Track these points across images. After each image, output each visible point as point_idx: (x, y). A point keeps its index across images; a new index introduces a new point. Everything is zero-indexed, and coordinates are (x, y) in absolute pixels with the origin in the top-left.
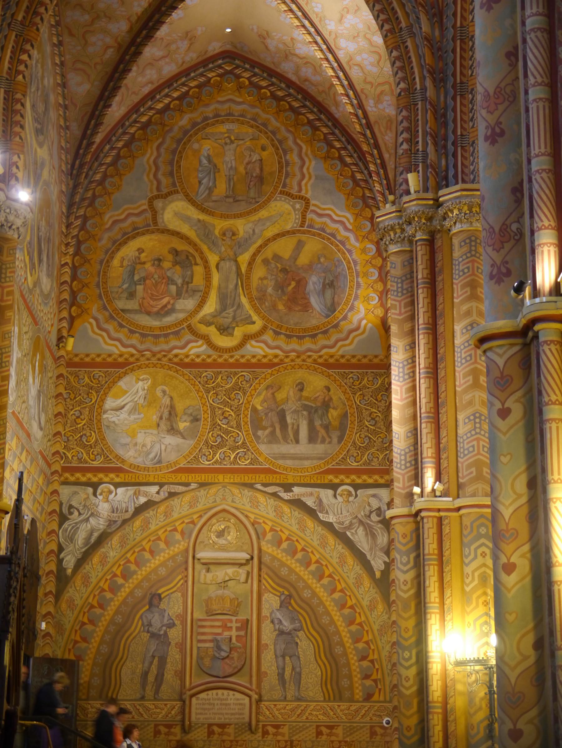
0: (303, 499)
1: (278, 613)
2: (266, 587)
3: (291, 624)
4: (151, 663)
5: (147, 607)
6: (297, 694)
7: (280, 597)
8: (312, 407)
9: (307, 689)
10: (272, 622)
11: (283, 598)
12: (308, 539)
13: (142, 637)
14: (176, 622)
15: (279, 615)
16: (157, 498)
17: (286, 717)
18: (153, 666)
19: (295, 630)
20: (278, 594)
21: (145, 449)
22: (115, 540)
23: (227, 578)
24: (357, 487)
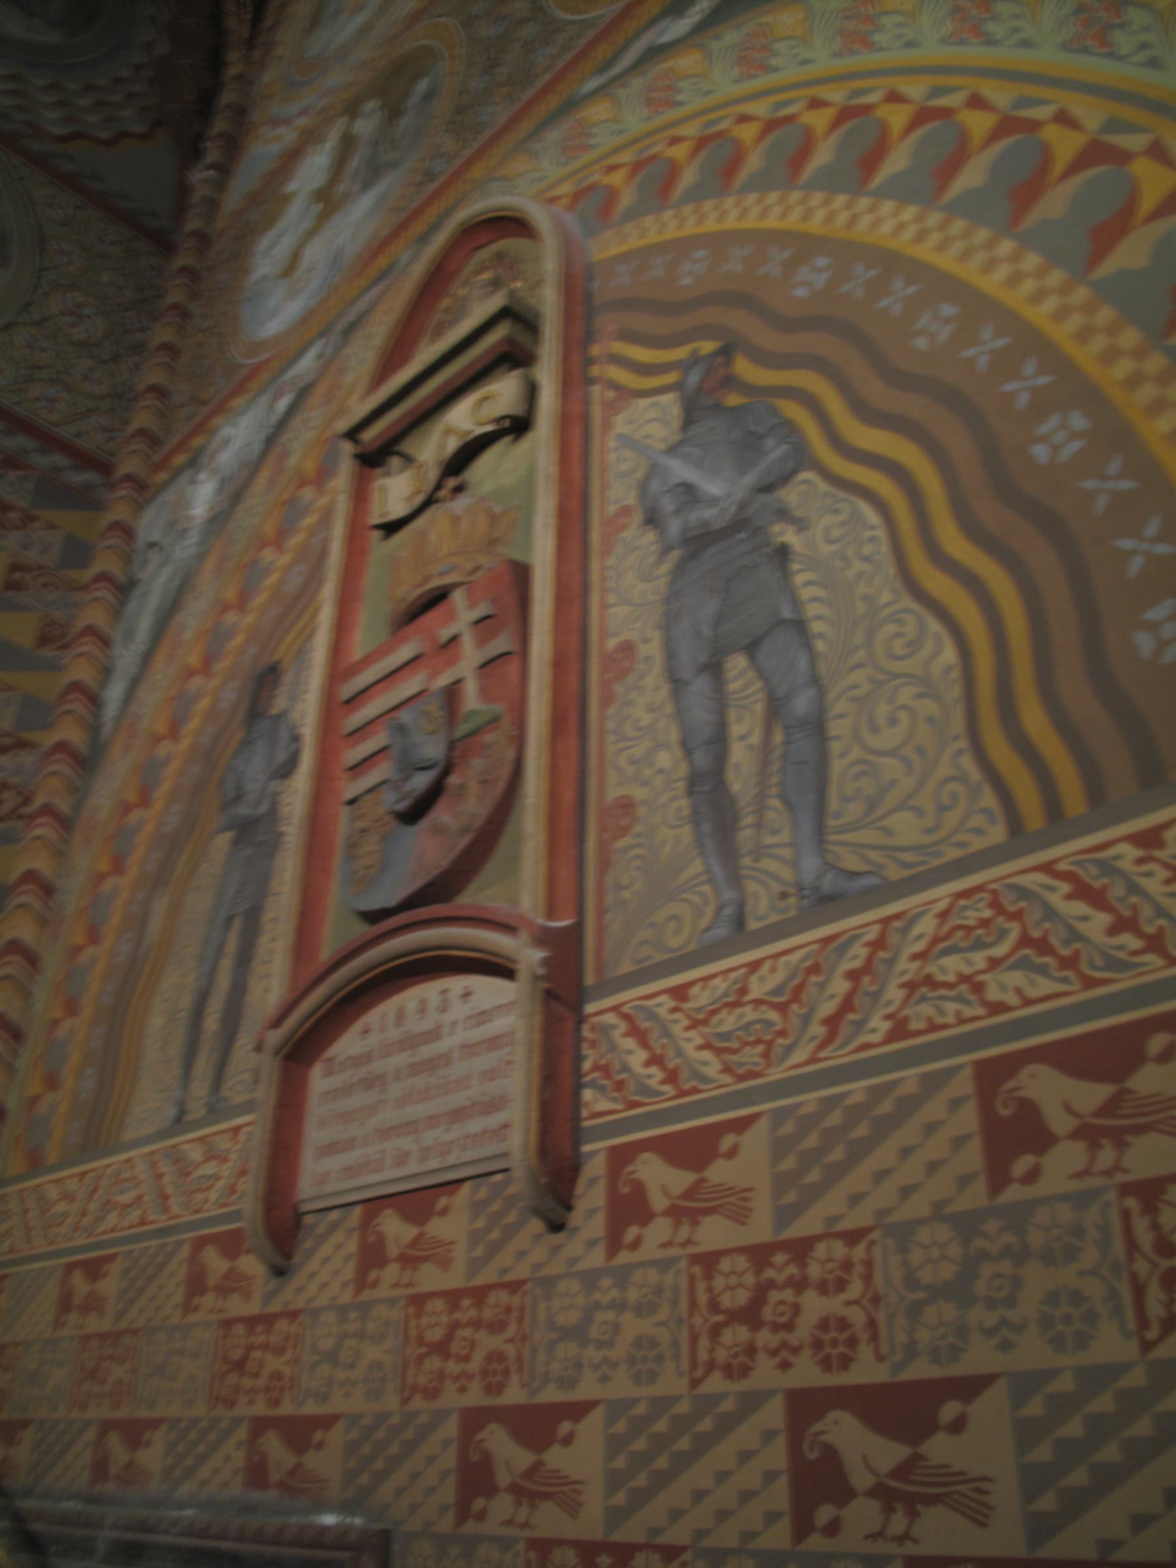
6: (810, 864)
9: (872, 805)
15: (681, 471)
17: (751, 1056)
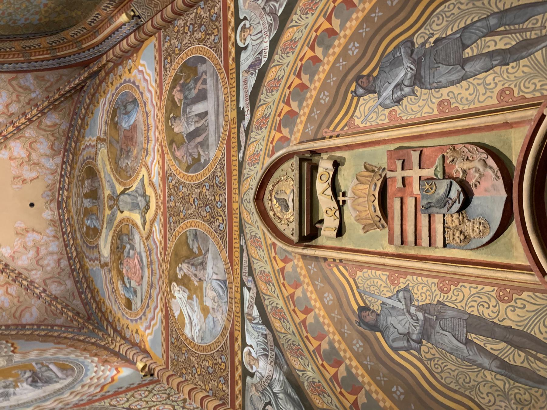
0: (249, 93)
1: (384, 94)
2: (346, 125)
3: (401, 63)
4: (481, 350)
5: (379, 334)
7: (359, 97)
8: (184, 103)
10: (398, 101)
11: (361, 91)
12: (287, 70)
13: (429, 356)
14: (402, 286)
15: (387, 92)
16: (254, 291)
18: (488, 347)
19: (412, 51)
20: (356, 99)
21: (216, 299)
22: (296, 364)
23: (329, 192)
24: (238, 21)
